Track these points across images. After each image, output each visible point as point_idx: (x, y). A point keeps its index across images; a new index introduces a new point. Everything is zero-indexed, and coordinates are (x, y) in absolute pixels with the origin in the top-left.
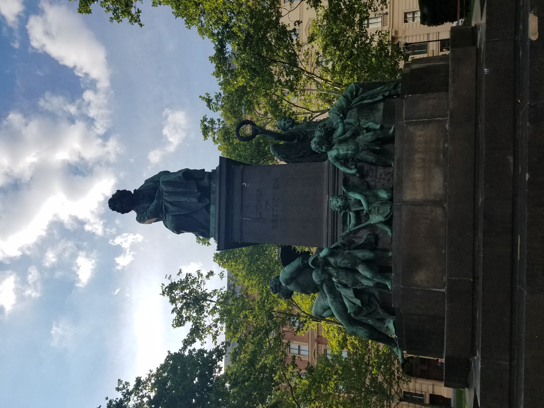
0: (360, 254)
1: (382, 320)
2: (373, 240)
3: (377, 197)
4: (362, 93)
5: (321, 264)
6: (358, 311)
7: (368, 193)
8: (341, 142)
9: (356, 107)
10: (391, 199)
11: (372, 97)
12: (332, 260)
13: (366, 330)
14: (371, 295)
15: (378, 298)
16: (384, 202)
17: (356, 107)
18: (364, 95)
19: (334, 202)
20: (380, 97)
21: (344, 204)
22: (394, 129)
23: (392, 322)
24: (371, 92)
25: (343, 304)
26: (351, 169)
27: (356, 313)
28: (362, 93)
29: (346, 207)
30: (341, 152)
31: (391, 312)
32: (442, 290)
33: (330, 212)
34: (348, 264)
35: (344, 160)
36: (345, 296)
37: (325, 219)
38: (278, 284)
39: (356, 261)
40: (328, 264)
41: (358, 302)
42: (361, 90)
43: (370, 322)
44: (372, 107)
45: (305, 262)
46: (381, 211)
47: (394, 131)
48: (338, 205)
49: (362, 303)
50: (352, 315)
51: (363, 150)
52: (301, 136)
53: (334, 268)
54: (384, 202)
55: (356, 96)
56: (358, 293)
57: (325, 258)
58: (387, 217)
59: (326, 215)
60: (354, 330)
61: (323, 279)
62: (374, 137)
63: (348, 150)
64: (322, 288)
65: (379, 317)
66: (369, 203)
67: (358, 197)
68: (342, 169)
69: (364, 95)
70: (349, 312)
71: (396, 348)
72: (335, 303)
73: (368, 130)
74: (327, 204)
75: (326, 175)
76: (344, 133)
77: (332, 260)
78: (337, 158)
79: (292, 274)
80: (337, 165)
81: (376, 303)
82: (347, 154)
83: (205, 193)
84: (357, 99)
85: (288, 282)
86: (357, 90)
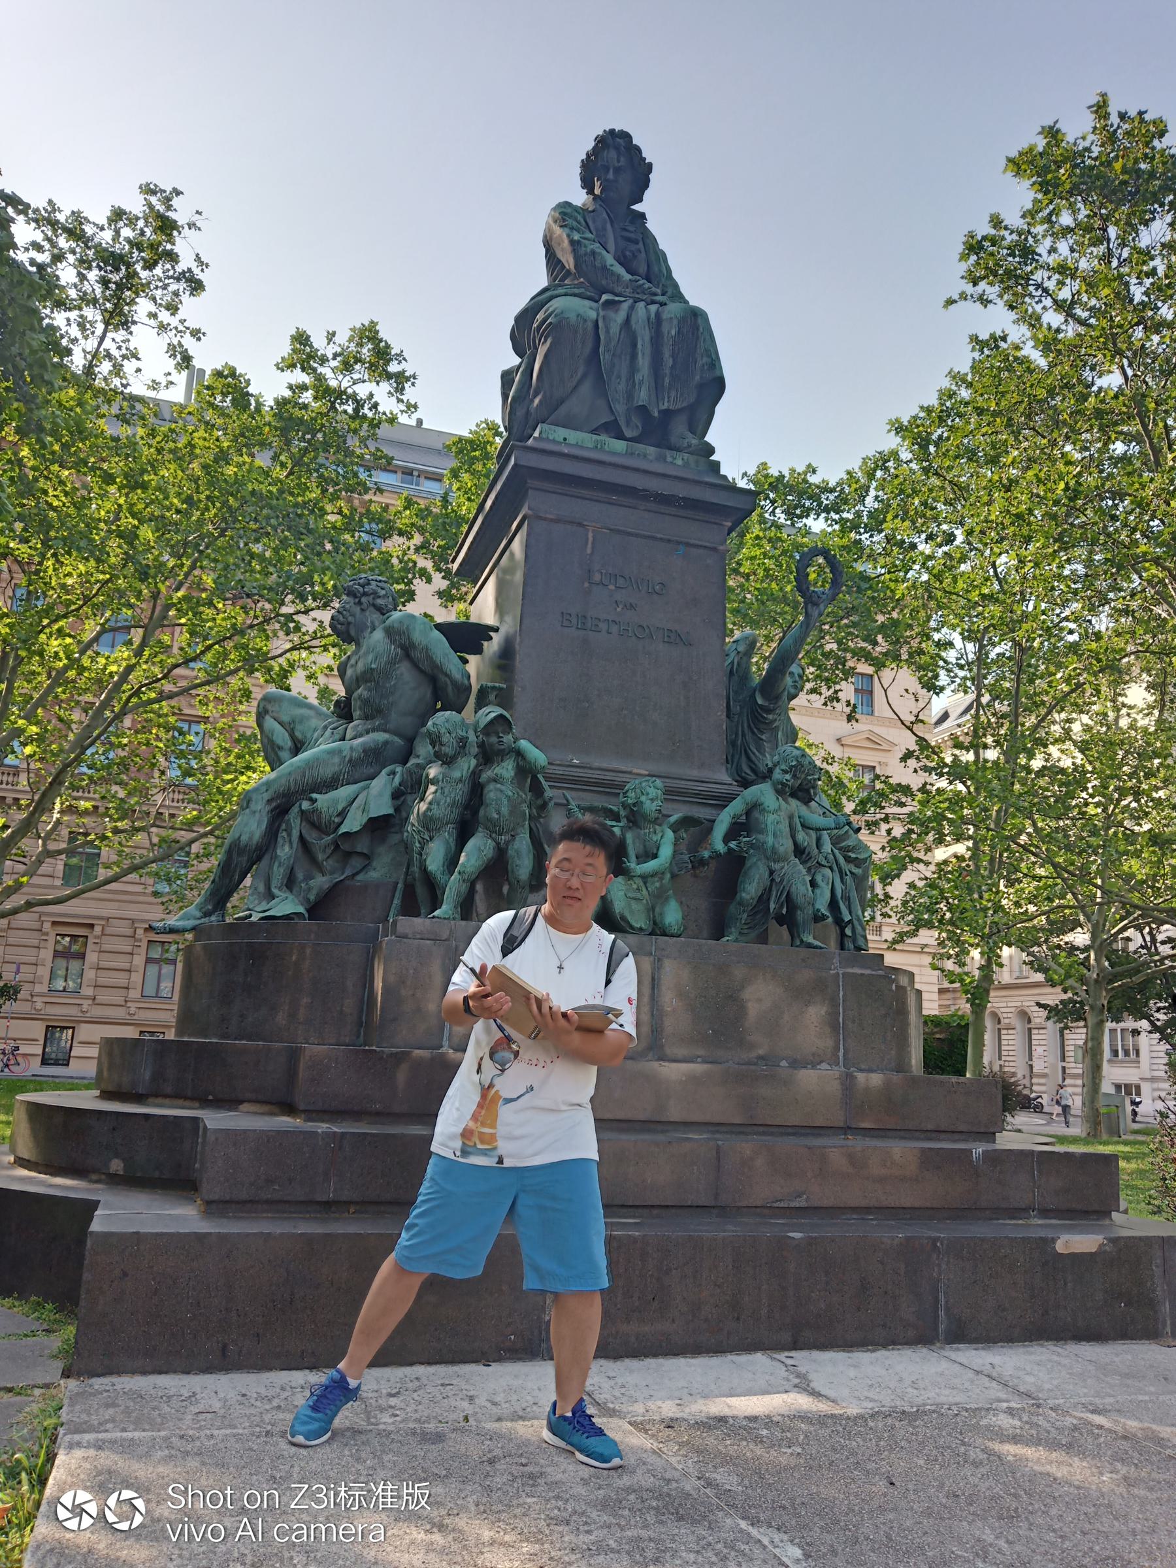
1: (290, 883)
5: (494, 739)
7: (668, 876)
12: (506, 769)
13: (257, 836)
15: (360, 877)
19: (652, 792)
20: (847, 918)
21: (645, 817)
22: (816, 947)
23: (301, 909)
25: (331, 784)
26: (727, 839)
29: (635, 817)
30: (771, 818)
32: (445, 1042)
33: (619, 778)
34: (499, 813)
36: (367, 787)
38: (379, 601)
40: (488, 756)
41: (353, 823)
43: (285, 851)
45: (492, 697)
46: (635, 906)
47: (810, 946)
48: (643, 798)
51: (771, 873)
52: (770, 717)
53: (475, 774)
55: (848, 860)
56: (378, 826)
58: (623, 918)
59: (596, 764)
61: (444, 740)
62: (800, 900)
63: (775, 835)
64: (374, 730)
65: (300, 875)
66: (644, 878)
67: (666, 852)
69: (848, 879)
70: (314, 796)
71: (198, 914)
72: (336, 760)
74: (624, 768)
75: (695, 773)
77: (506, 769)
80: (736, 807)
81: (348, 872)
82: (762, 831)
83: (656, 429)
84: (841, 860)
86: (857, 862)
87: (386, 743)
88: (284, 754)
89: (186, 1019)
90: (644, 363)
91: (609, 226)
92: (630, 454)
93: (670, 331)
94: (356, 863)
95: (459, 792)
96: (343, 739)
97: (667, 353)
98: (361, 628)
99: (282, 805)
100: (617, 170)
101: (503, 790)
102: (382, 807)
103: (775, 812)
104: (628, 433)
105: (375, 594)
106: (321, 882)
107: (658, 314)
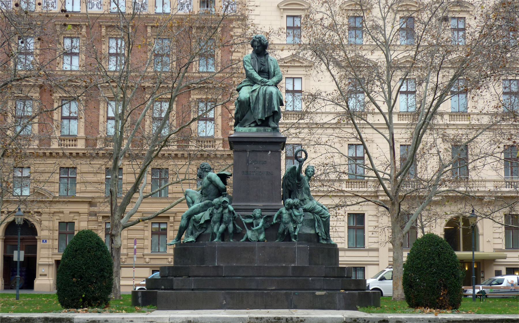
0: (231, 226)
1: (192, 234)
2: (238, 232)
3: (260, 234)
4: (322, 220)
6: (197, 221)
7: (263, 229)
8: (290, 215)
9: (314, 218)
10: (259, 241)
11: (319, 226)
12: (226, 211)
14: (206, 228)
16: (257, 238)
17: (314, 218)
18: (321, 222)
19: (258, 212)
23: (193, 240)
24: (322, 226)
27: (195, 220)
28: (322, 220)
29: (255, 218)
30: (284, 215)
31: (198, 239)
35: (280, 217)
37: (248, 204)
39: (227, 223)
40: (225, 208)
41: (202, 222)
42: (324, 220)
43: (190, 227)
44: (313, 227)
49: (201, 224)
50: (193, 218)
53: (222, 211)
54: (257, 238)
55: (321, 217)
56: (207, 222)
57: (227, 207)
60: (184, 218)
62: (290, 232)
65: (194, 232)
66: (257, 230)
67: (261, 224)
68: (276, 214)
69: (321, 222)
73: (295, 228)
76: (295, 216)
78: (281, 213)
79: (215, 182)
83: (264, 123)
85: (209, 179)
87: (209, 203)
88: (191, 205)
89: (175, 262)
90: (261, 107)
91: (257, 63)
92: (257, 131)
93: (267, 97)
94: (204, 230)
95: (219, 215)
96: (201, 202)
97: (266, 102)
98: (203, 176)
99: (189, 217)
100: (258, 47)
101: (226, 216)
102: (207, 217)
103: (285, 213)
104: (259, 124)
105: (205, 168)
106: (198, 233)
107: (265, 91)
